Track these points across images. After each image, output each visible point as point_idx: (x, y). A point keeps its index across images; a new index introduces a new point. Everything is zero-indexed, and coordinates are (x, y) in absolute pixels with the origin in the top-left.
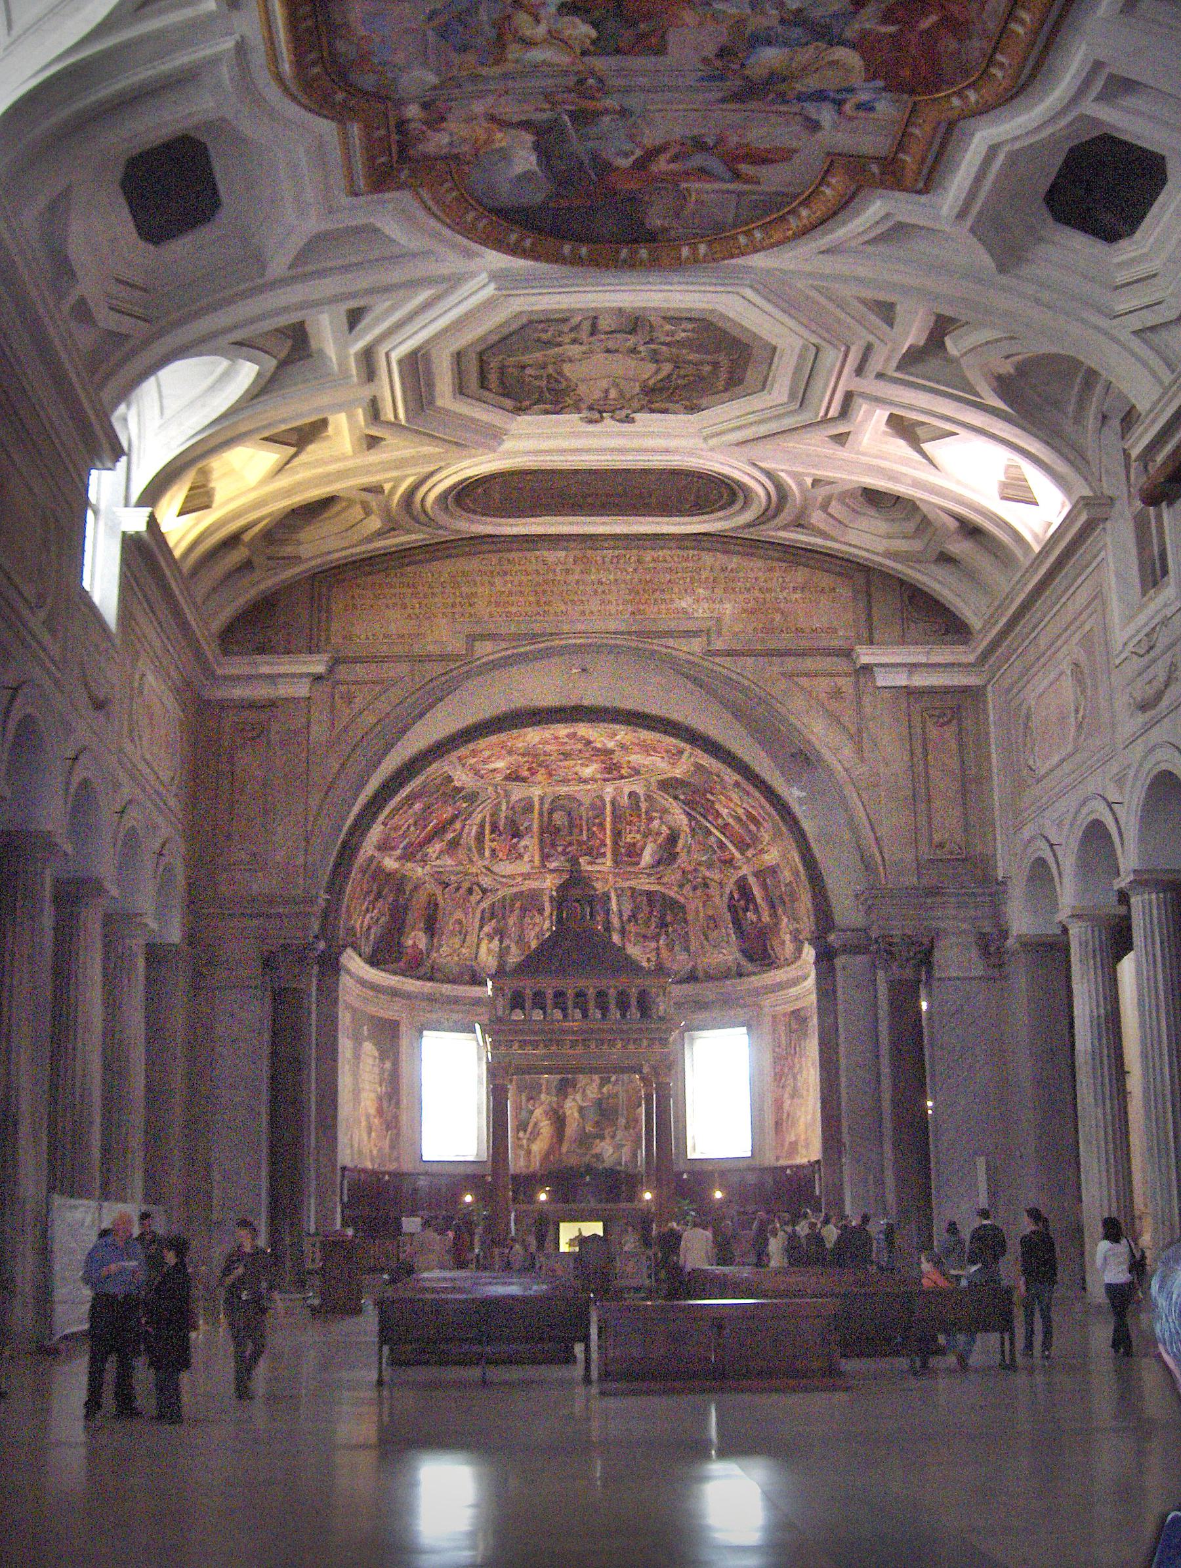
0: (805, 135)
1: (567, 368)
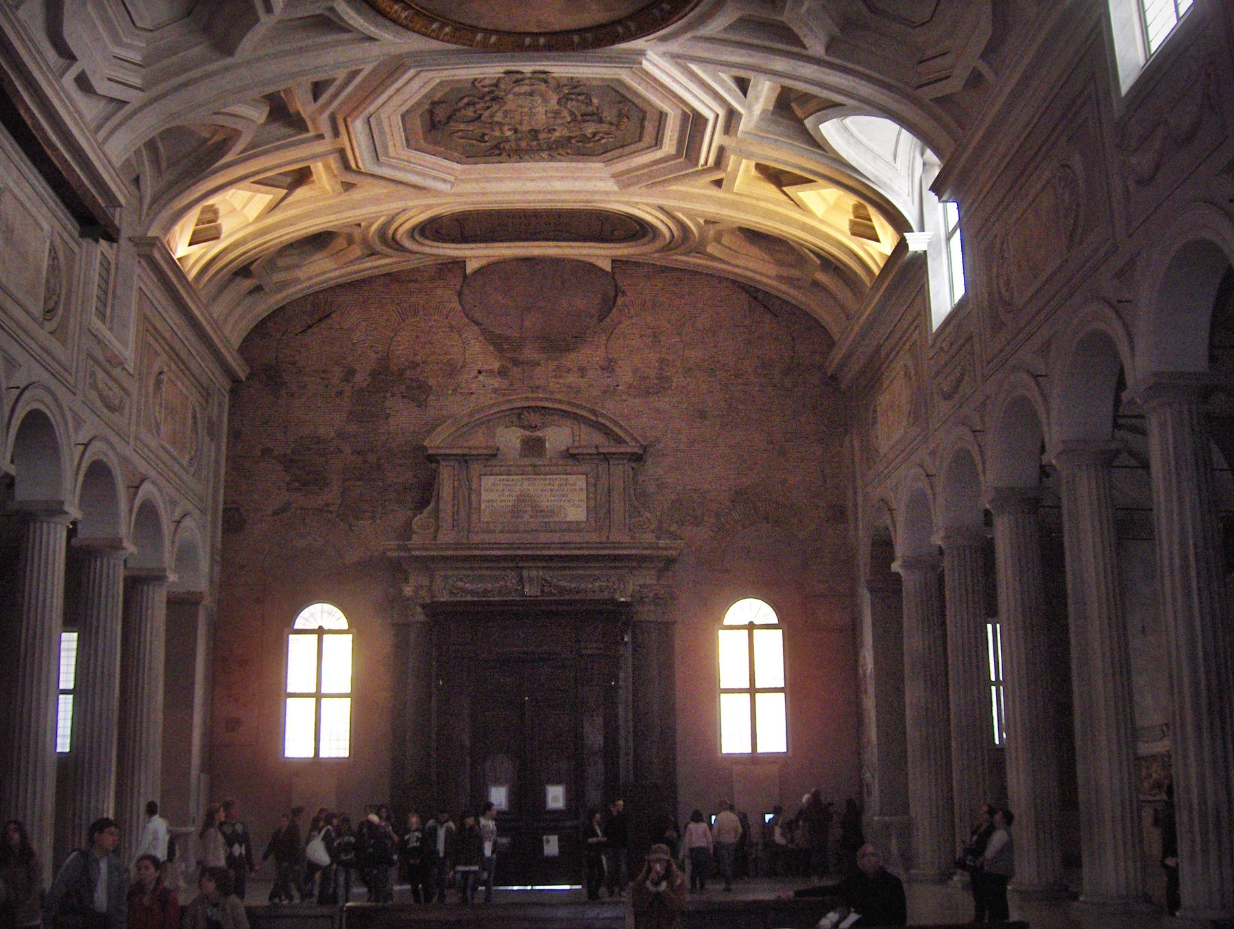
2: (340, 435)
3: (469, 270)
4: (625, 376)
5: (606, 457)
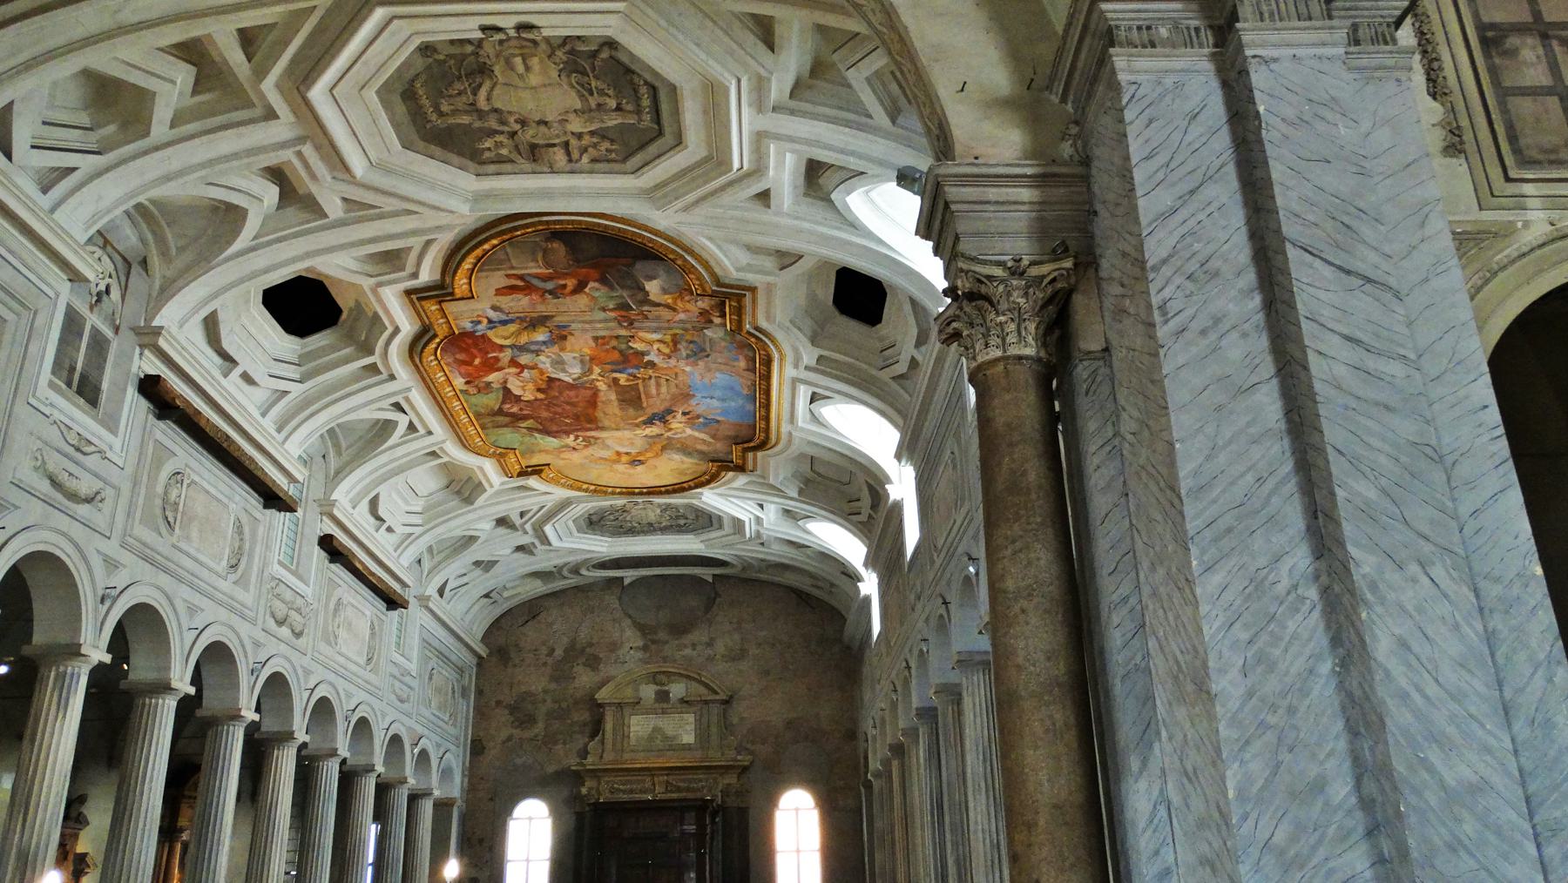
0: (498, 304)
1: (579, 105)
2: (545, 691)
3: (627, 582)
4: (720, 648)
5: (706, 702)
